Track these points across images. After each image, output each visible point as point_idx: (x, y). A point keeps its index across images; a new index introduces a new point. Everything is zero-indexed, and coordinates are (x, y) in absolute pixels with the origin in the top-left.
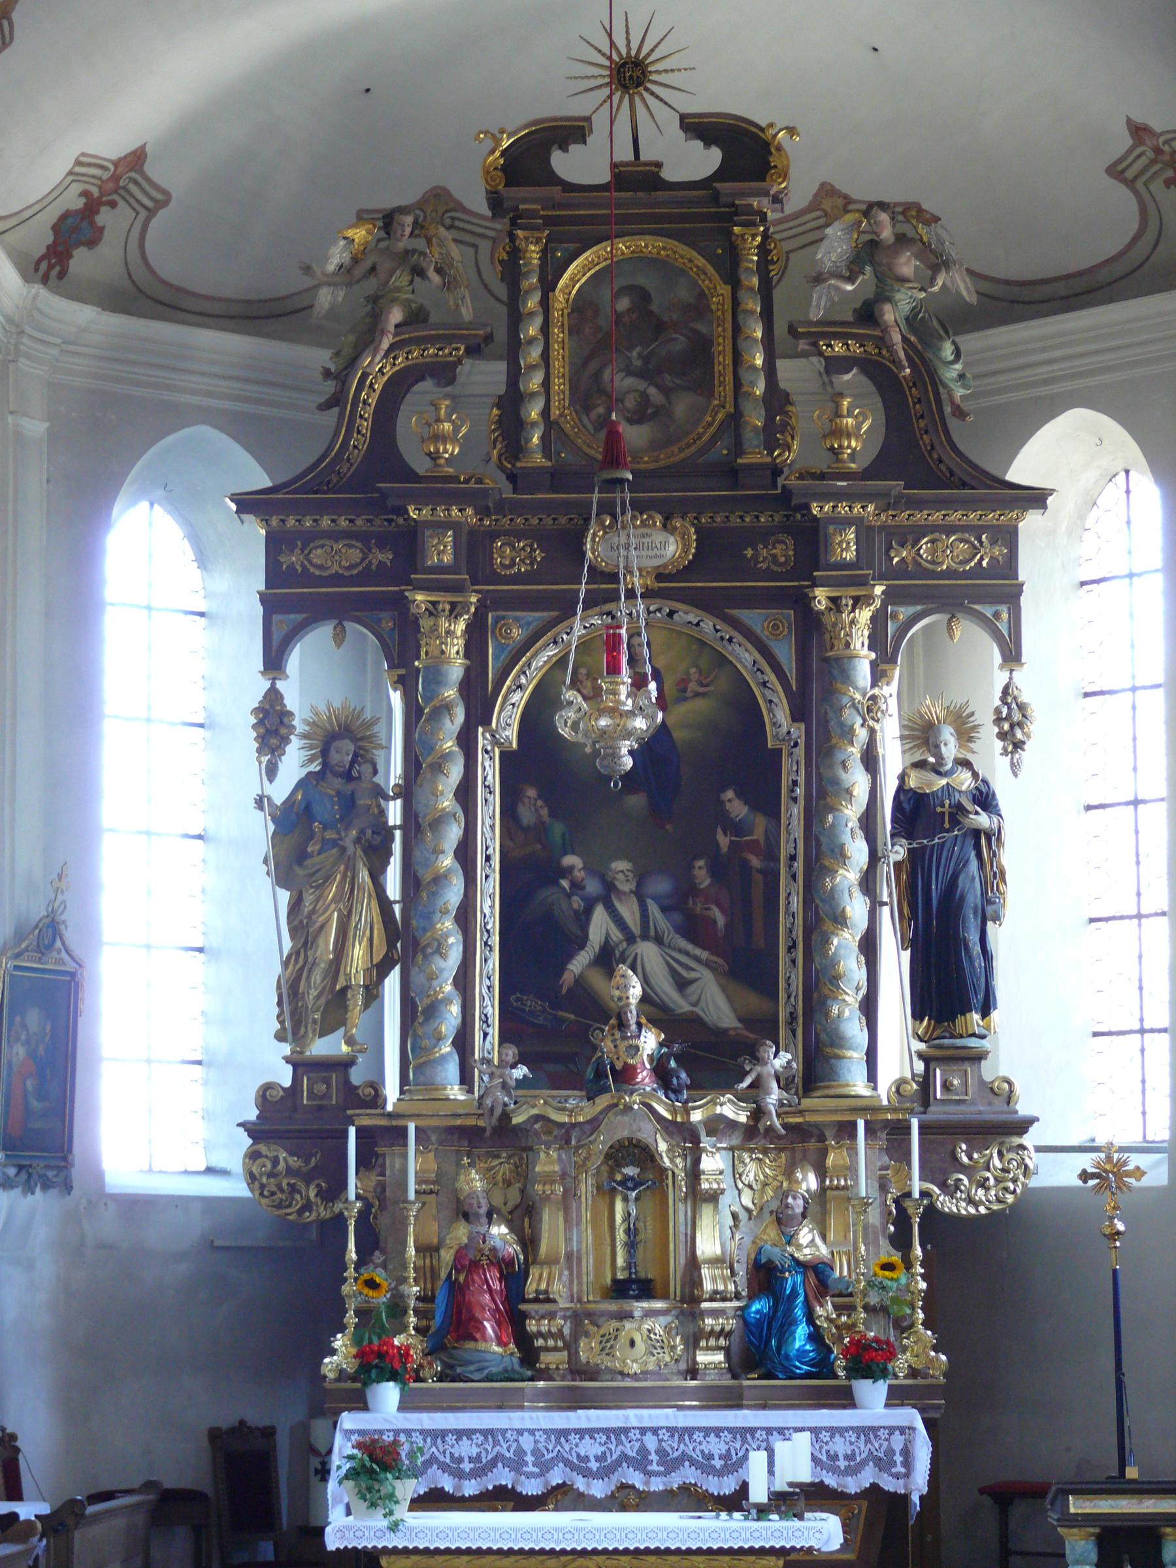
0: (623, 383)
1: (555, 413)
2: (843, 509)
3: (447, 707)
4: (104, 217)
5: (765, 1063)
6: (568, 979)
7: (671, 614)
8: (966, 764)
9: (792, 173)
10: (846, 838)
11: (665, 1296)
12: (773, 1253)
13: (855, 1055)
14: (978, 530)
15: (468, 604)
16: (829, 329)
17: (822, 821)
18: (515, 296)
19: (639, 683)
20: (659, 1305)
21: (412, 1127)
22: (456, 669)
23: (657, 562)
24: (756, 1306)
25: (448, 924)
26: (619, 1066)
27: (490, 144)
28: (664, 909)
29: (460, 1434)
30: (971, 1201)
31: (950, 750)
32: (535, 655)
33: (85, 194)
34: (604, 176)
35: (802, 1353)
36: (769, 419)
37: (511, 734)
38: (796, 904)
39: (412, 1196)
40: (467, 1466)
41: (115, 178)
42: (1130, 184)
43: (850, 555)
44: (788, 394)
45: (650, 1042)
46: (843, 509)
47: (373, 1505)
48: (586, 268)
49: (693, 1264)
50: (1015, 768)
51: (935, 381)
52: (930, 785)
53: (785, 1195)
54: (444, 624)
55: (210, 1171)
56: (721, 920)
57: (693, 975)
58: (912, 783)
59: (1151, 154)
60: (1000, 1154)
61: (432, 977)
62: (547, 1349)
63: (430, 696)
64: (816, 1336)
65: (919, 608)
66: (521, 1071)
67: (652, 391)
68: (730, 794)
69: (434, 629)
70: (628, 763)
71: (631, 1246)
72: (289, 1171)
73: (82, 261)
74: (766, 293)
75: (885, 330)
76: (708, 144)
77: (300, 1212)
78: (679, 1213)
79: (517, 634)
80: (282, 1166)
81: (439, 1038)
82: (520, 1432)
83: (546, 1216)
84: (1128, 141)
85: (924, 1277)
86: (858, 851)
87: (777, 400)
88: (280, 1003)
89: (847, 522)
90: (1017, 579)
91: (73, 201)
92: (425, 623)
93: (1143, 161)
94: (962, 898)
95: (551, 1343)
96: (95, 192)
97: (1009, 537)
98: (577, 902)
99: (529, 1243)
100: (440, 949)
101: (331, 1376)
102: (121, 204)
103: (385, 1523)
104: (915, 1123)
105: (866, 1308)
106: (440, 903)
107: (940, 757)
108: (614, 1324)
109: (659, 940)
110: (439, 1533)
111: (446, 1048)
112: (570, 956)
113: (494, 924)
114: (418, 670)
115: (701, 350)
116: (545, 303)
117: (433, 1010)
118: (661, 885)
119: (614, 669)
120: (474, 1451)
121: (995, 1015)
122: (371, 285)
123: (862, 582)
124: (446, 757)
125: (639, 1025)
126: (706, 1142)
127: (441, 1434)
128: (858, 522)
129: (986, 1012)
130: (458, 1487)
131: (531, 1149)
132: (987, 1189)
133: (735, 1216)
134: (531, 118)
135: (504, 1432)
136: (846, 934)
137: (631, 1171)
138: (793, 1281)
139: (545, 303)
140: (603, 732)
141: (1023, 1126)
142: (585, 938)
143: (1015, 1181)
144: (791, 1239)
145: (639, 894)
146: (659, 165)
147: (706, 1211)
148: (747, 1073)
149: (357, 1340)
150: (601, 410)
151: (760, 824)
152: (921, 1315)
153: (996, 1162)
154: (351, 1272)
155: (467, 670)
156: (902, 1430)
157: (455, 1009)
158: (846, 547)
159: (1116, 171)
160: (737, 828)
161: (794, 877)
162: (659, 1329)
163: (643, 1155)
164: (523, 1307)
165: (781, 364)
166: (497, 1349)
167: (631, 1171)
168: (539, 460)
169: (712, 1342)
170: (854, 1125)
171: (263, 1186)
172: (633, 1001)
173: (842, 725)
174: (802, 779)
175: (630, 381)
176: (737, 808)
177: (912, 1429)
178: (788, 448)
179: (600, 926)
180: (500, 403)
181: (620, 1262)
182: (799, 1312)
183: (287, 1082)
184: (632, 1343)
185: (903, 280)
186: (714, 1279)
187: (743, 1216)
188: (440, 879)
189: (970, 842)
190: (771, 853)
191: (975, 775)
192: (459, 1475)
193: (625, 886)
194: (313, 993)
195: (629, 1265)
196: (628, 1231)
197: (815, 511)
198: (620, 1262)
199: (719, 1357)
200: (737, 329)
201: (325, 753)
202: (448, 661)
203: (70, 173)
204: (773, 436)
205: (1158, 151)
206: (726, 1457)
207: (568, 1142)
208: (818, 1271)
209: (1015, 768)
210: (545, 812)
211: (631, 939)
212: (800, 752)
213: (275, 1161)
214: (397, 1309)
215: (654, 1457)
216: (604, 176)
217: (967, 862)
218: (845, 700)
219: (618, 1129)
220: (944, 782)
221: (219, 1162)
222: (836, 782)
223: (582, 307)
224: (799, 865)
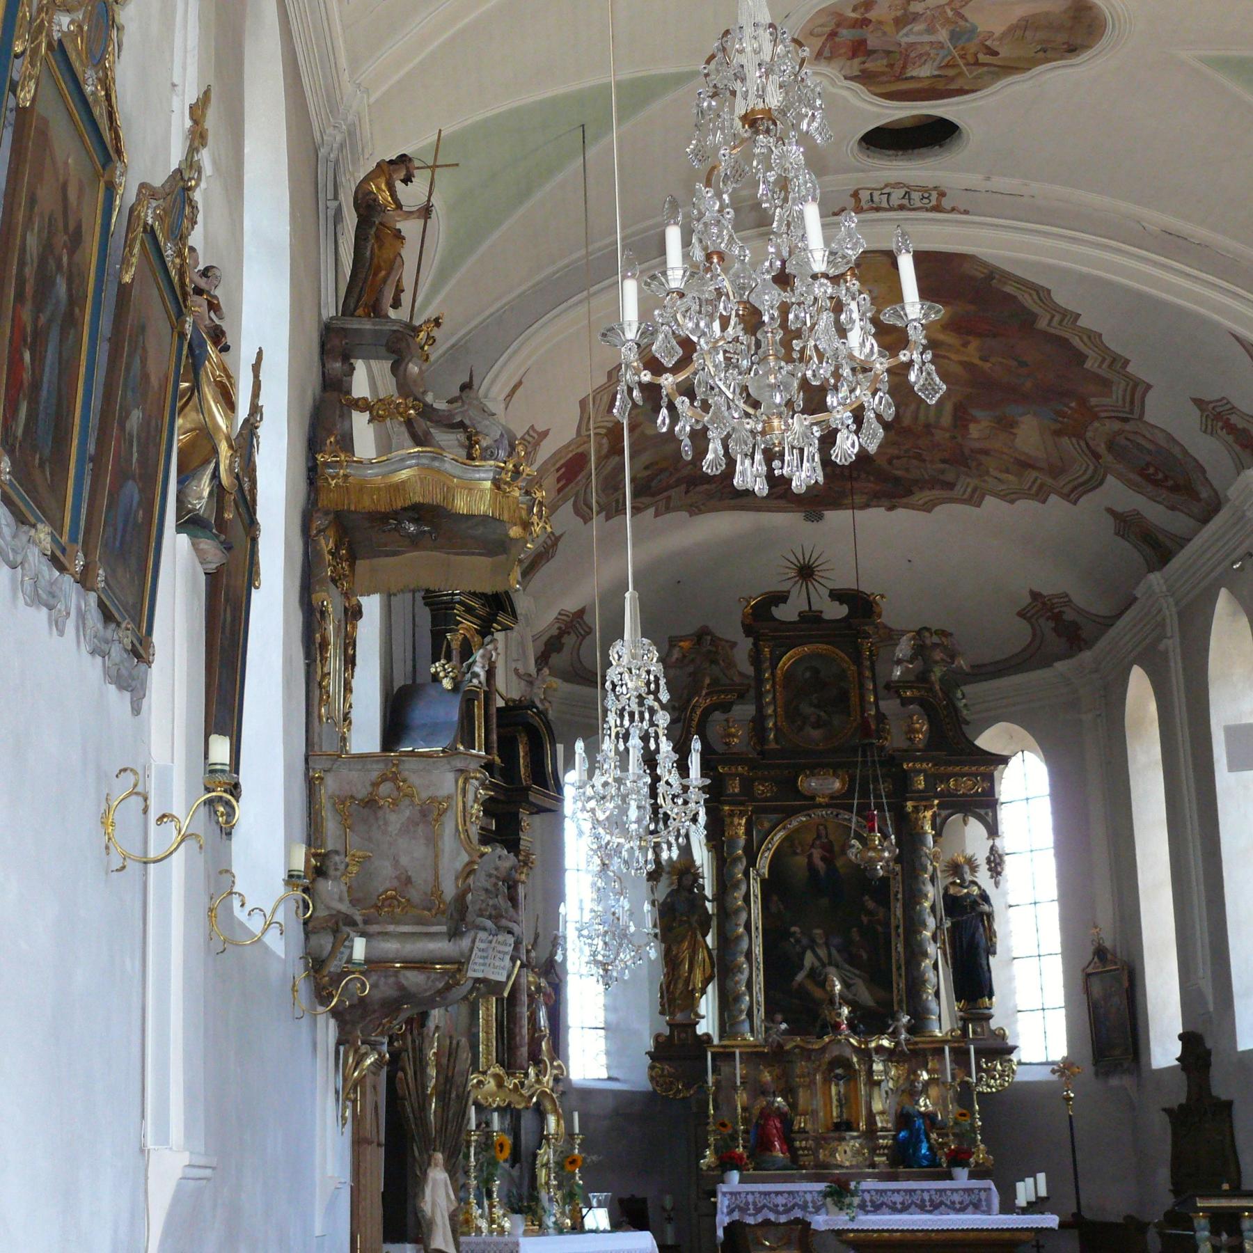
0: (807, 709)
1: (779, 724)
2: (918, 766)
3: (739, 859)
4: (565, 639)
5: (898, 1020)
6: (795, 984)
7: (837, 815)
8: (975, 883)
9: (884, 613)
10: (927, 917)
11: (858, 1130)
12: (908, 1108)
13: (933, 1017)
14: (976, 775)
15: (747, 811)
16: (904, 684)
17: (914, 909)
18: (759, 671)
19: (885, 837)
20: (855, 1134)
21: (737, 1052)
22: (742, 841)
23: (830, 791)
24: (902, 1134)
25: (742, 959)
26: (833, 1022)
27: (746, 604)
28: (839, 951)
29: (777, 1193)
30: (989, 1086)
31: (968, 877)
32: (775, 835)
33: (559, 628)
34: (795, 618)
35: (925, 1156)
36: (878, 726)
37: (765, 871)
38: (901, 948)
39: (738, 1084)
40: (781, 1209)
41: (572, 621)
42: (1028, 620)
43: (922, 786)
44: (884, 715)
45: (845, 1011)
46: (918, 766)
47: (841, 1209)
48: (789, 659)
49: (871, 1117)
50: (997, 884)
51: (956, 710)
52: (960, 892)
53: (913, 1082)
54: (736, 821)
55: (610, 1079)
56: (865, 956)
57: (851, 982)
58: (952, 891)
59: (1040, 605)
60: (1001, 1065)
61: (737, 983)
62: (802, 1155)
63: (730, 854)
64: (930, 1148)
65: (950, 811)
66: (784, 1026)
67: (822, 714)
68: (867, 898)
69: (732, 822)
70: (881, 873)
71: (841, 1105)
72: (670, 1075)
73: (555, 659)
74: (872, 669)
75: (932, 684)
76: (841, 603)
77: (675, 1094)
78: (863, 1090)
79: (767, 825)
80: (666, 1072)
81: (741, 1012)
82: (805, 1192)
83: (801, 1094)
84: (1029, 600)
85: (980, 1119)
86: (931, 922)
87: (881, 717)
88: (662, 997)
89: (919, 772)
90: (994, 796)
91: (555, 632)
92: (728, 820)
93: (1036, 609)
94: (978, 943)
95: (806, 1152)
96: (563, 626)
97: (990, 779)
98: (798, 949)
99: (793, 1106)
100: (740, 970)
101: (705, 1168)
102: (572, 634)
103: (847, 1218)
104: (972, 1048)
105: (954, 1135)
106: (739, 949)
107: (963, 880)
108: (836, 1143)
109: (837, 966)
110: (874, 1222)
111: (744, 1016)
112: (796, 974)
113: (761, 959)
114: (723, 842)
115: (844, 697)
116: (773, 674)
117: (738, 998)
118: (836, 940)
119: (872, 830)
120: (784, 1201)
121: (994, 999)
122: (691, 669)
123: (927, 799)
124: (739, 881)
125: (840, 1004)
126: (875, 1058)
127: (769, 1193)
128: (924, 771)
129: (990, 998)
130: (776, 1218)
131: (791, 1062)
132: (996, 1080)
133: (887, 1092)
134: (767, 590)
135: (798, 1192)
136: (927, 961)
137: (839, 1071)
138: (919, 1122)
139: (773, 674)
140: (871, 858)
141: (1011, 1050)
142: (803, 965)
143: (1008, 1076)
144: (917, 1103)
145: (827, 944)
146: (821, 612)
147: (876, 1091)
148: (890, 1026)
149: (716, 1151)
150: (799, 723)
151: (881, 912)
152: (979, 1137)
153: (999, 1067)
154: (711, 1120)
155: (747, 841)
156: (985, 1190)
157: (747, 998)
158: (920, 783)
159: (1021, 614)
160: (870, 913)
161: (899, 936)
162: (857, 1145)
163: (847, 1064)
164: (793, 1135)
165: (881, 703)
166: (781, 1155)
167: (839, 1071)
168: (773, 746)
169: (882, 1151)
170: (943, 1050)
171: (657, 1082)
172: (837, 992)
173: (921, 865)
174: (900, 890)
175: (813, 709)
176: (870, 904)
177: (990, 1189)
178: (886, 739)
179: (809, 959)
180: (753, 720)
181: (835, 1114)
182: (923, 1137)
183: (668, 1033)
184: (845, 1152)
185: (936, 662)
186: (882, 1122)
187: (890, 1092)
188: (739, 938)
189: (979, 919)
190: (887, 924)
191: (979, 888)
192: (778, 1213)
193: (820, 941)
194: (678, 991)
195: (840, 1116)
196: (839, 1100)
197: (905, 767)
198: (835, 1114)
199: (884, 1159)
200: (862, 686)
201: (680, 880)
202: (739, 837)
203: (556, 618)
204: (881, 733)
205: (1044, 604)
206: (902, 1203)
207: (810, 1058)
208: (929, 1117)
209: (997, 884)
210: (782, 907)
211: (824, 965)
212: (899, 878)
213: (663, 1070)
214: (733, 1137)
215: (869, 1204)
216: (795, 618)
217: (978, 927)
218: (922, 853)
219: (835, 1051)
220: (965, 891)
221: (615, 1074)
222: (920, 891)
223: (789, 676)
224: (901, 930)
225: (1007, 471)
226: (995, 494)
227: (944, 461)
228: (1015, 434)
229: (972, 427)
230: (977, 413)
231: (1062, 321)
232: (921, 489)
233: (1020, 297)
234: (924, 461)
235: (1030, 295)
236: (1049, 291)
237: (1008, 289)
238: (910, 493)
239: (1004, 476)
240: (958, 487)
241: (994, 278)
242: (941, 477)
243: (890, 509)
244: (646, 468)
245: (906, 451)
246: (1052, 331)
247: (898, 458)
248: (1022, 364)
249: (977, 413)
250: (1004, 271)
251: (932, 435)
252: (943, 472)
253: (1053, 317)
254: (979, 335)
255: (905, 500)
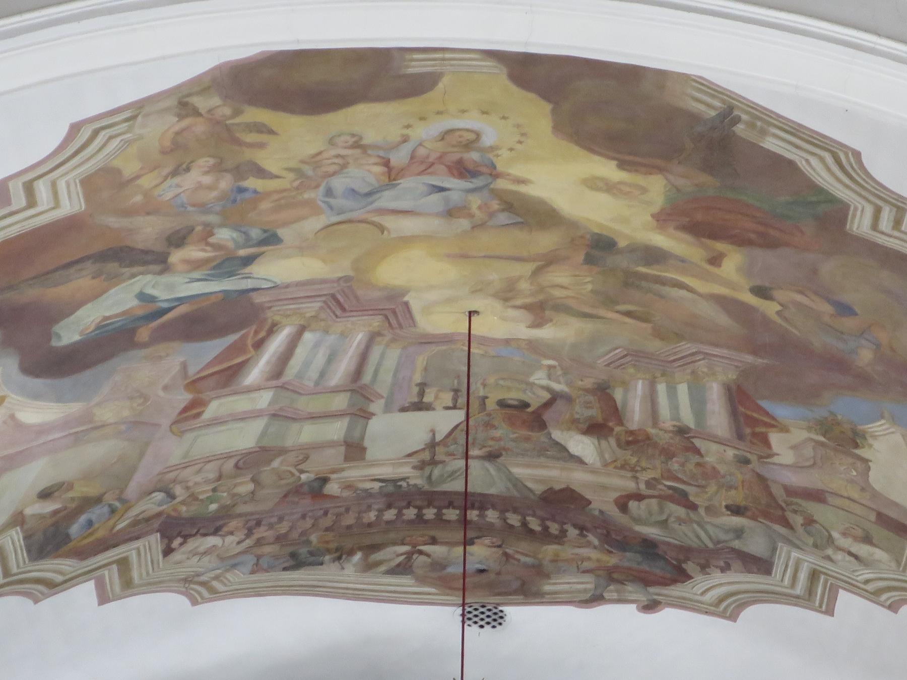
225: (867, 539)
226: (853, 588)
227: (736, 510)
228: (866, 461)
229: (775, 438)
230: (781, 411)
231: (897, 223)
232: (704, 568)
233: (802, 165)
234: (693, 507)
235: (822, 160)
236: (857, 155)
237: (771, 144)
238: (681, 576)
239: (863, 550)
240: (777, 570)
241: (737, 120)
242: (736, 544)
243: (651, 607)
244: (45, 495)
245: (649, 484)
246: (881, 240)
247: (639, 497)
248: (845, 310)
249: (781, 411)
250: (754, 106)
251: (697, 452)
252: (739, 533)
253: (878, 211)
254: (741, 241)
255: (676, 591)
